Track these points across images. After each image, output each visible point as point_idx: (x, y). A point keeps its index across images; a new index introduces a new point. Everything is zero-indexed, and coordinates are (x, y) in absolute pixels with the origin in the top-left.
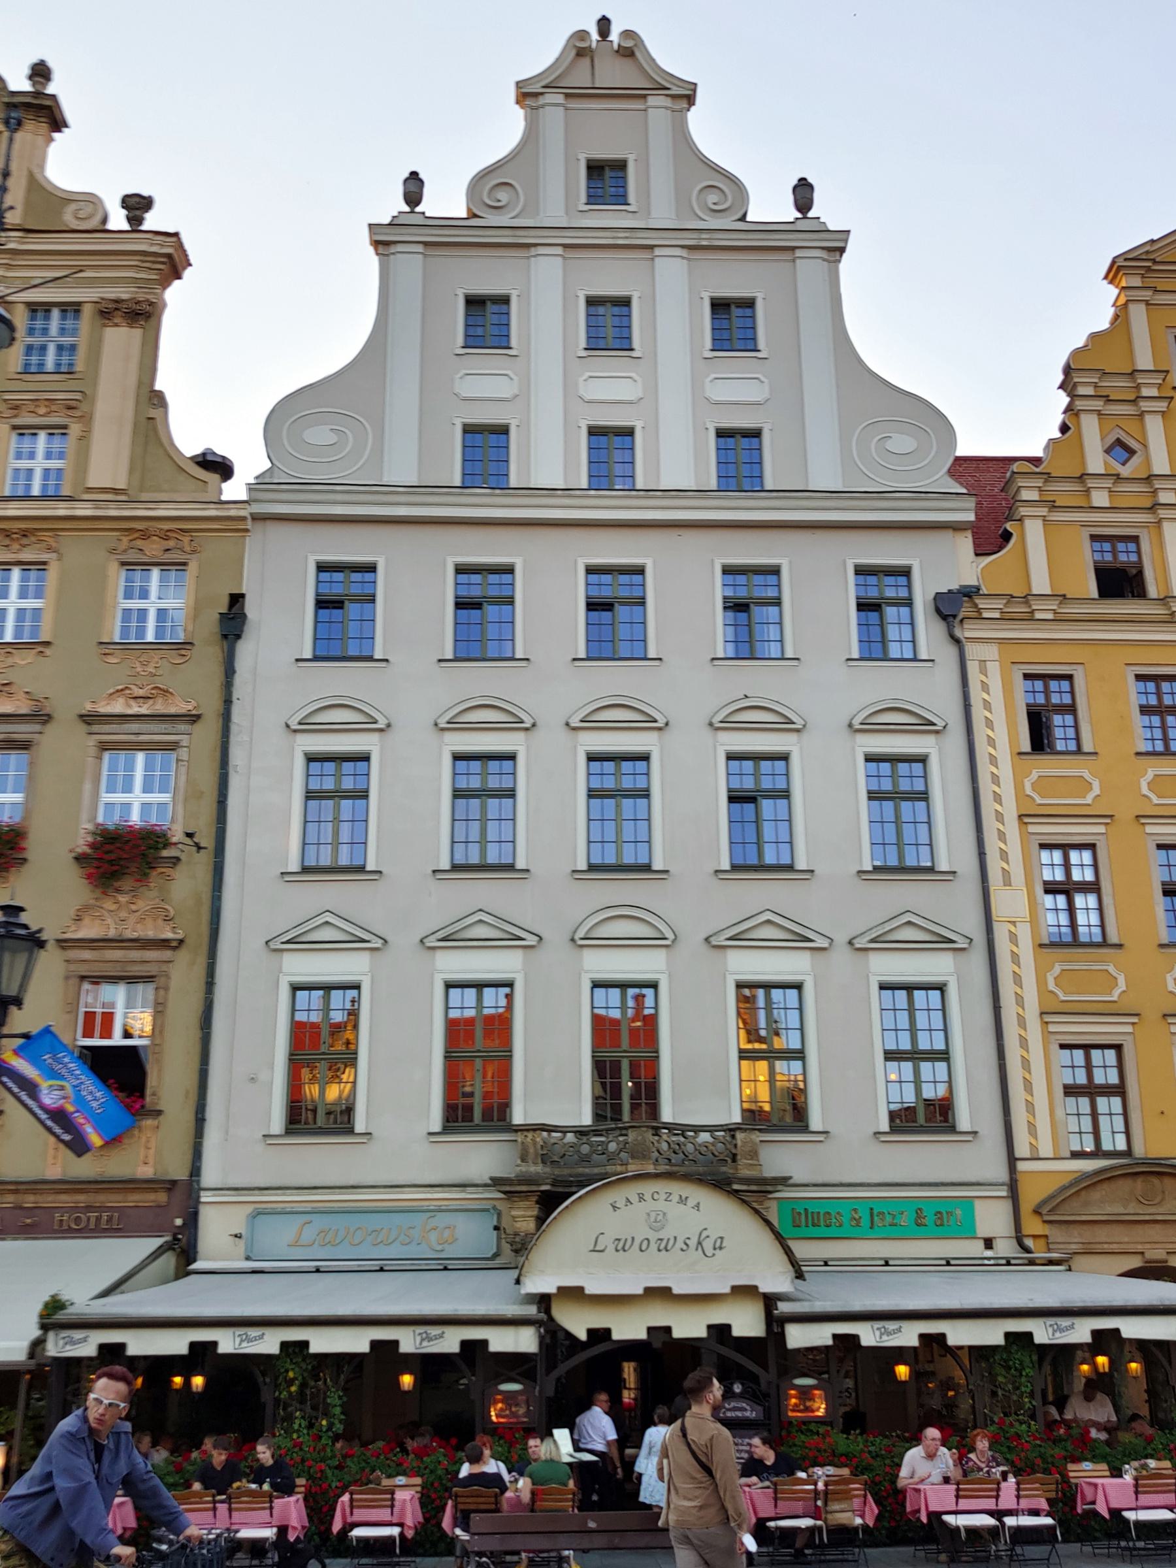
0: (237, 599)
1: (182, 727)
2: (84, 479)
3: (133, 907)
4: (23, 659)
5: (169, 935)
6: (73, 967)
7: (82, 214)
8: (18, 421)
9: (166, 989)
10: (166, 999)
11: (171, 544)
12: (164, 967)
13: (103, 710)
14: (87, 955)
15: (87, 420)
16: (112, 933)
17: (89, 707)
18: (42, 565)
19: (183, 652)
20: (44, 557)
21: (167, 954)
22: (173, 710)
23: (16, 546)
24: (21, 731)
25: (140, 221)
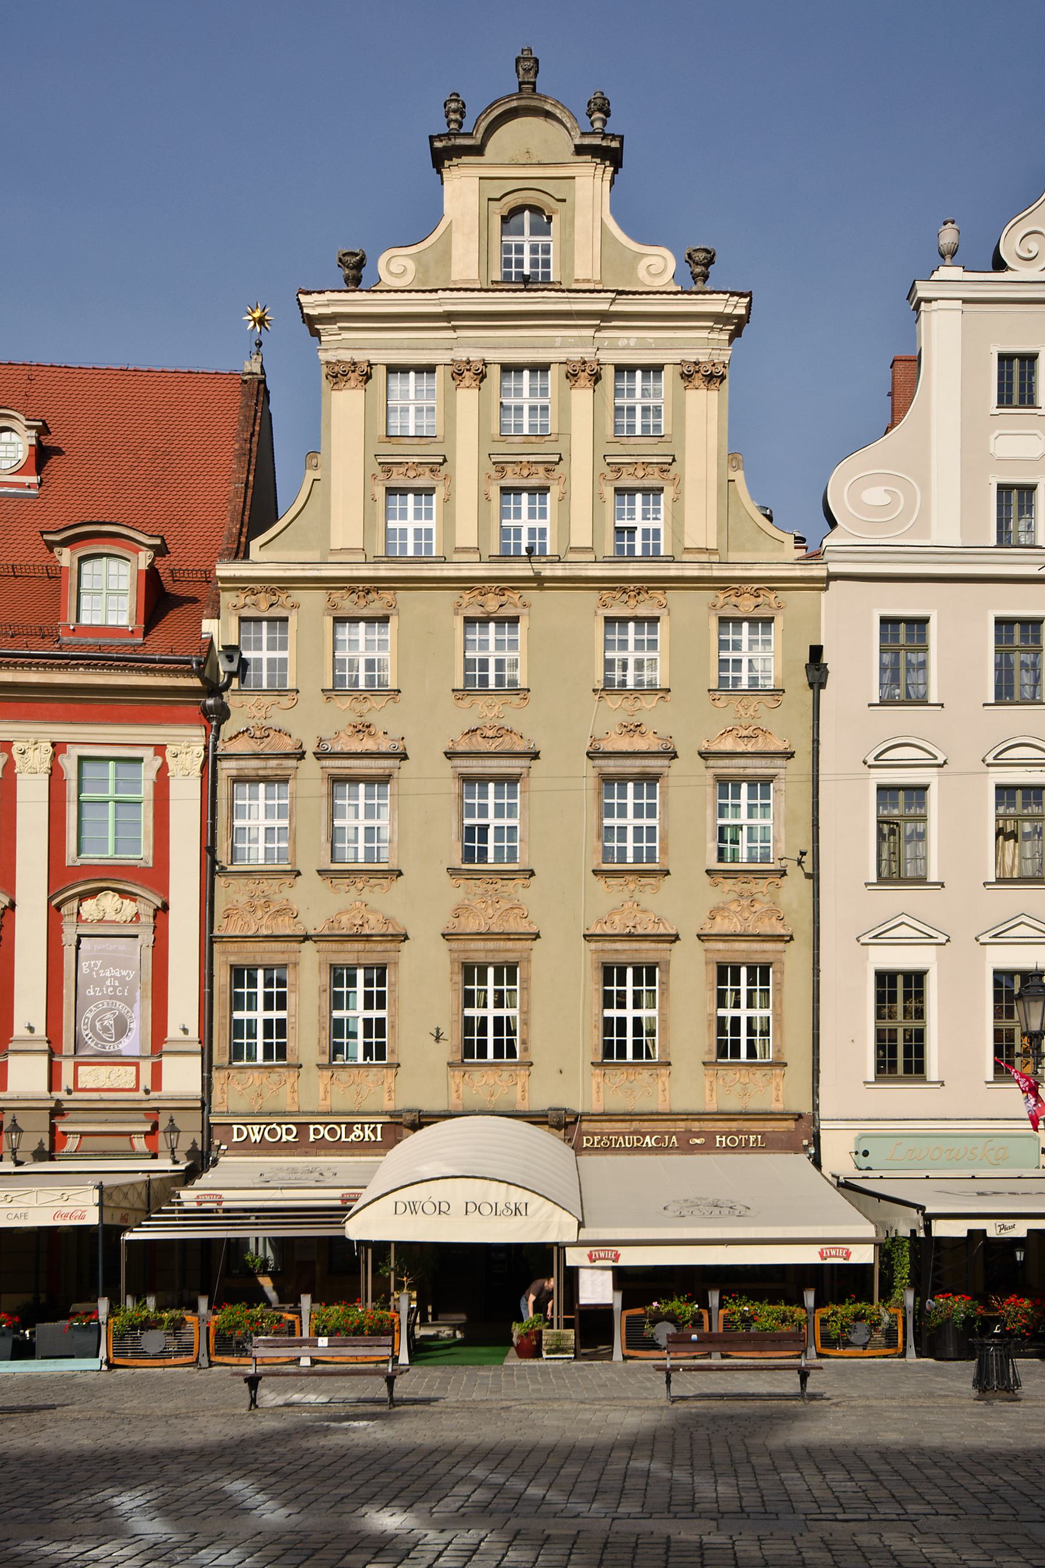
0: (816, 652)
1: (779, 762)
2: (681, 541)
3: (753, 909)
4: (649, 702)
5: (782, 932)
6: (710, 955)
7: (653, 270)
8: (620, 484)
9: (782, 973)
10: (782, 980)
11: (760, 600)
12: (779, 956)
13: (715, 747)
14: (720, 946)
15: (678, 482)
16: (739, 930)
17: (704, 746)
18: (654, 620)
19: (776, 698)
20: (656, 613)
21: (780, 946)
22: (772, 748)
23: (632, 602)
24: (653, 765)
25: (706, 277)
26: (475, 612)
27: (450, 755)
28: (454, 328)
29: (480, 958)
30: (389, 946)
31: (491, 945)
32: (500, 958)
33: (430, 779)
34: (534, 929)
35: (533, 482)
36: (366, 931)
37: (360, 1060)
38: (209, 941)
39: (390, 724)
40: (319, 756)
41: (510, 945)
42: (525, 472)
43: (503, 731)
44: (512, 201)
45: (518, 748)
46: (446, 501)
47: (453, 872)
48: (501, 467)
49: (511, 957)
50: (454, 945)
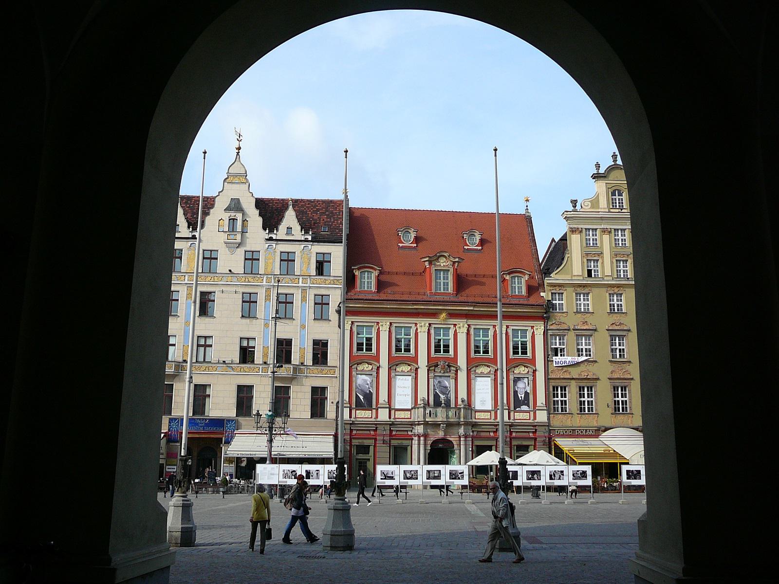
26: (612, 292)
27: (608, 330)
28: (602, 220)
29: (617, 384)
30: (595, 381)
31: (620, 381)
32: (623, 385)
33: (603, 337)
34: (631, 377)
35: (624, 259)
36: (589, 377)
37: (587, 412)
38: (547, 380)
39: (592, 322)
40: (574, 330)
41: (625, 381)
42: (622, 256)
43: (621, 324)
44: (614, 188)
45: (625, 329)
46: (602, 263)
47: (611, 361)
48: (616, 255)
49: (626, 384)
50: (611, 381)
